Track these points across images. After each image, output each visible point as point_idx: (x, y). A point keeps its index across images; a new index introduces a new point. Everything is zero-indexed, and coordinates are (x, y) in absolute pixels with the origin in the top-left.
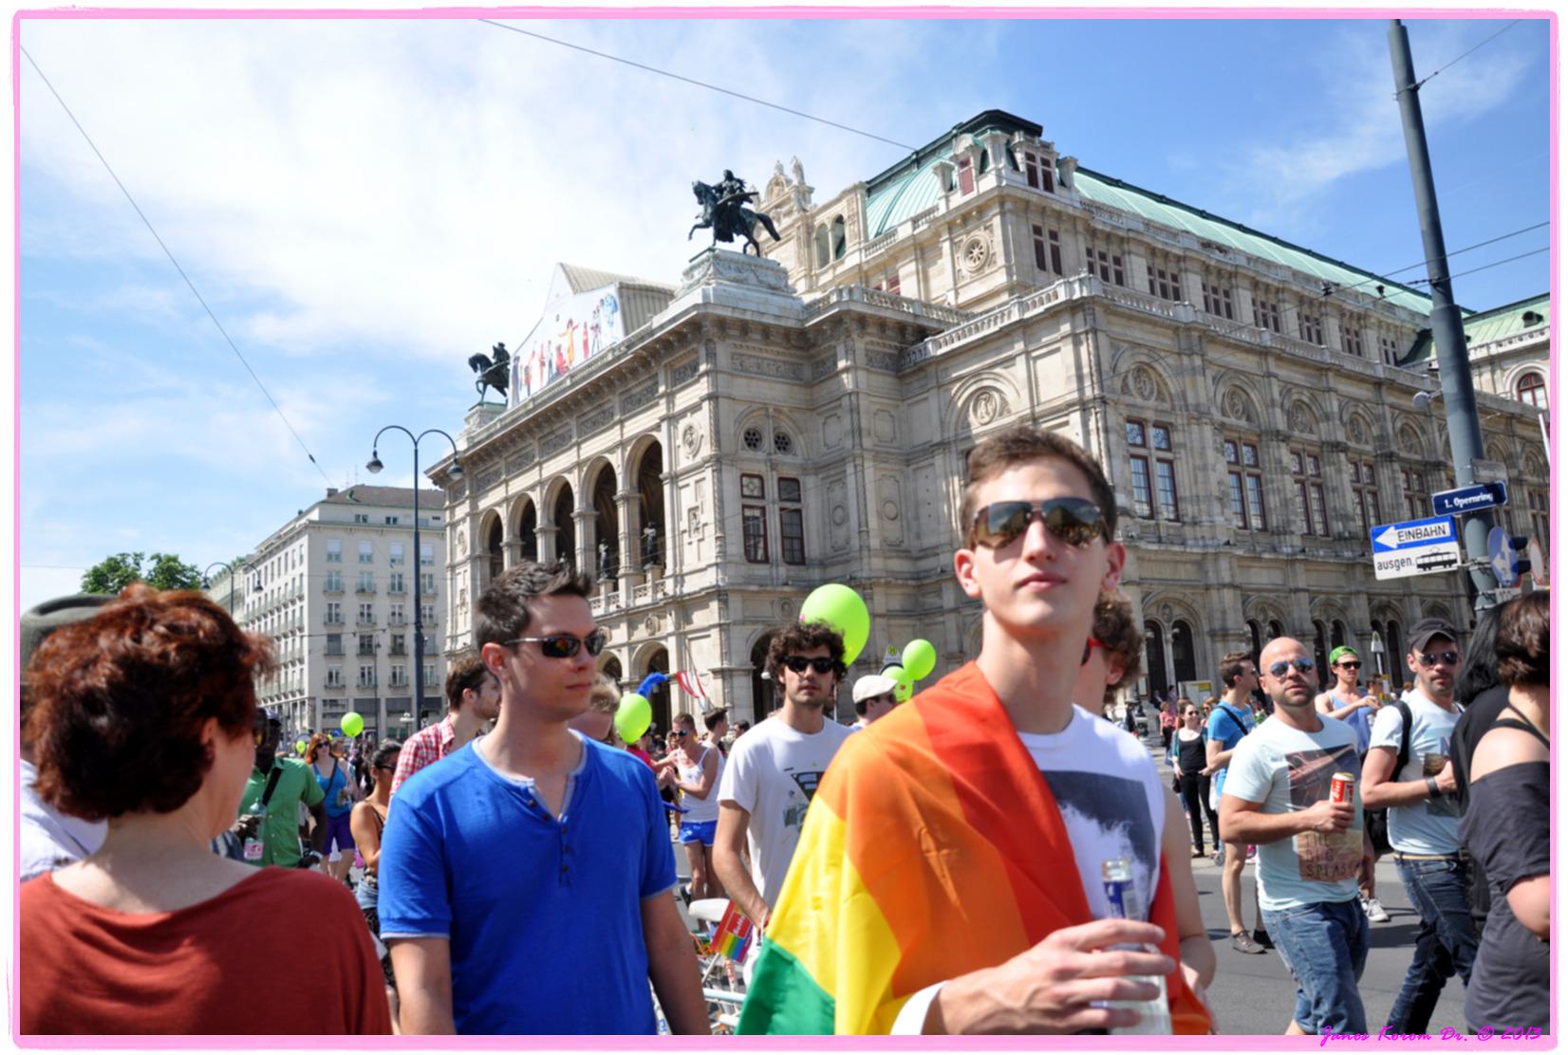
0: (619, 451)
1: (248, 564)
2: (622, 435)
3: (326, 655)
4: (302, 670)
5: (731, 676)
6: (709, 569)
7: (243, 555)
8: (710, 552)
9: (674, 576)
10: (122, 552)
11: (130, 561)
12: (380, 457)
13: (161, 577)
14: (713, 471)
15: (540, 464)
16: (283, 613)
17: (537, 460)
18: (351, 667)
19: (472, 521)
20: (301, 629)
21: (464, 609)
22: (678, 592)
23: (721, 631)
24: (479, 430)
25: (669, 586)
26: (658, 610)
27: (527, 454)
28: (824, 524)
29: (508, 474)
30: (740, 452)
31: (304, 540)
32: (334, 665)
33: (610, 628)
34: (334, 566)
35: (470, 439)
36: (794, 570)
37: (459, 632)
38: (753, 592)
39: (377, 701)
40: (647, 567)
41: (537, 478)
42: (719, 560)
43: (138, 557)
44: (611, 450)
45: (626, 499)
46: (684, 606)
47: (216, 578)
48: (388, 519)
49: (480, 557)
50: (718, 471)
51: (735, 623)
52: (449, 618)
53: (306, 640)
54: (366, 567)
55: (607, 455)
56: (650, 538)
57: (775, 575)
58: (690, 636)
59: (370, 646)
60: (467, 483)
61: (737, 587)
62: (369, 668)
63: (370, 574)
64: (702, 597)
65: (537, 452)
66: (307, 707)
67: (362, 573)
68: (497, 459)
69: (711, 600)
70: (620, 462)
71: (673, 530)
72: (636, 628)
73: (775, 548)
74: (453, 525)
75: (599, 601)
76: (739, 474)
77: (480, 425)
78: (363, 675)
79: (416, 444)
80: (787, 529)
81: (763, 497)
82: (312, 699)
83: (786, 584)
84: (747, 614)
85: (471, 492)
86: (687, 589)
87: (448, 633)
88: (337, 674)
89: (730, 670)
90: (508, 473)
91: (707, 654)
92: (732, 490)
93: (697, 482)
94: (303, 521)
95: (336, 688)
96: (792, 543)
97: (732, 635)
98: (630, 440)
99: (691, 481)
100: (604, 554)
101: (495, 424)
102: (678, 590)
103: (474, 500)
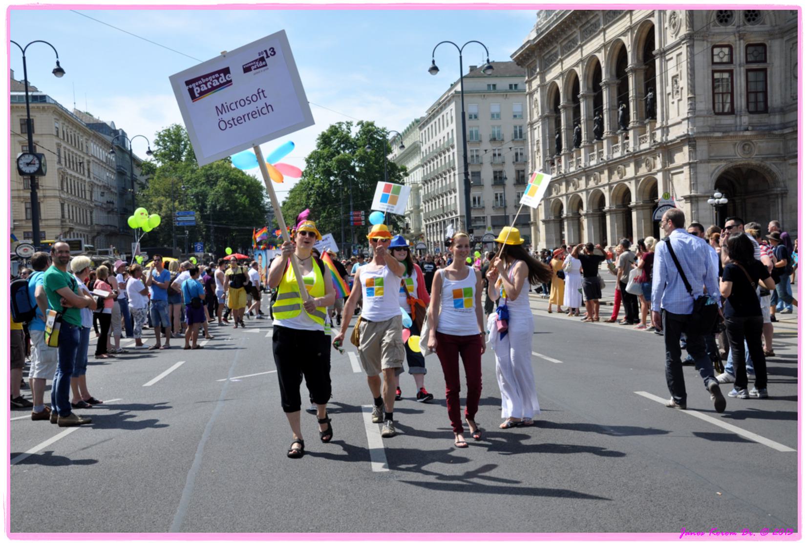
0: (629, 34)
1: (420, 124)
2: (631, 21)
4: (455, 197)
5: (697, 201)
6: (683, 122)
7: (418, 117)
8: (685, 109)
9: (662, 128)
10: (339, 121)
11: (344, 127)
12: (437, 64)
13: (364, 137)
14: (687, 46)
15: (581, 46)
16: (443, 158)
17: (579, 43)
19: (542, 91)
20: (454, 169)
22: (664, 140)
23: (690, 168)
24: (546, 21)
25: (658, 137)
26: (651, 152)
27: (573, 39)
28: (786, 78)
29: (562, 54)
30: (712, 28)
31: (453, 106)
33: (625, 166)
35: (537, 30)
36: (756, 118)
38: (718, 138)
40: (647, 121)
41: (580, 57)
42: (690, 115)
43: (349, 124)
44: (624, 34)
45: (634, 70)
46: (668, 150)
47: (403, 133)
48: (511, 86)
49: (547, 117)
50: (691, 47)
51: (701, 162)
52: (530, 161)
53: (457, 177)
54: (496, 122)
55: (622, 38)
56: (649, 100)
57: (738, 123)
58: (672, 172)
59: (501, 178)
60: (538, 63)
61: (703, 135)
62: (501, 194)
63: (499, 127)
65: (579, 38)
66: (459, 223)
67: (493, 127)
68: (555, 45)
69: (684, 145)
70: (630, 43)
71: (662, 94)
72: (641, 166)
73: (741, 102)
74: (531, 94)
75: (617, 147)
76: (710, 46)
77: (546, 17)
78: (497, 198)
79: (460, 52)
80: (752, 87)
81: (731, 62)
83: (747, 130)
84: (712, 155)
85: (541, 70)
86: (670, 138)
88: (479, 198)
89: (696, 197)
90: (562, 54)
91: (682, 185)
92: (702, 60)
93: (678, 55)
94: (453, 92)
96: (756, 98)
97: (698, 171)
98: (637, 24)
99: (674, 55)
100: (621, 112)
101: (553, 17)
102: (664, 138)
103: (543, 75)
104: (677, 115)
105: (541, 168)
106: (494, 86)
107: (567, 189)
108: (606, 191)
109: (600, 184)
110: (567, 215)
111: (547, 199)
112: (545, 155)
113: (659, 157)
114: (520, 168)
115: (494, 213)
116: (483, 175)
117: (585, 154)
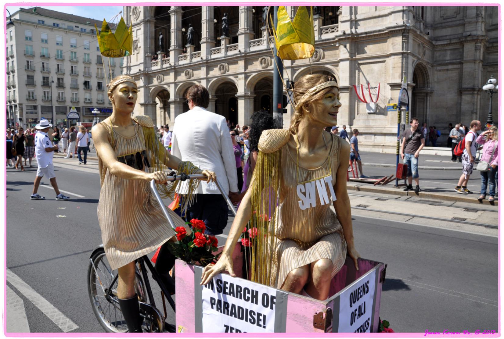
3: (26, 85)
4: (14, 91)
18: (39, 91)
20: (13, 72)
21: (136, 52)
32: (31, 89)
34: (29, 42)
37: (132, 65)
39: (52, 107)
48: (54, 24)
49: (148, 21)
59: (48, 82)
62: (48, 92)
64: (386, 33)
82: (20, 104)
87: (125, 65)
95: (31, 100)
104: (374, 10)
105: (142, 61)
106: (43, 22)
107: (176, 78)
108: (240, 79)
109: (227, 73)
110: (175, 100)
111: (146, 87)
112: (145, 52)
113: (345, 47)
114: (60, 77)
115: (43, 104)
116: (36, 78)
117: (207, 48)
